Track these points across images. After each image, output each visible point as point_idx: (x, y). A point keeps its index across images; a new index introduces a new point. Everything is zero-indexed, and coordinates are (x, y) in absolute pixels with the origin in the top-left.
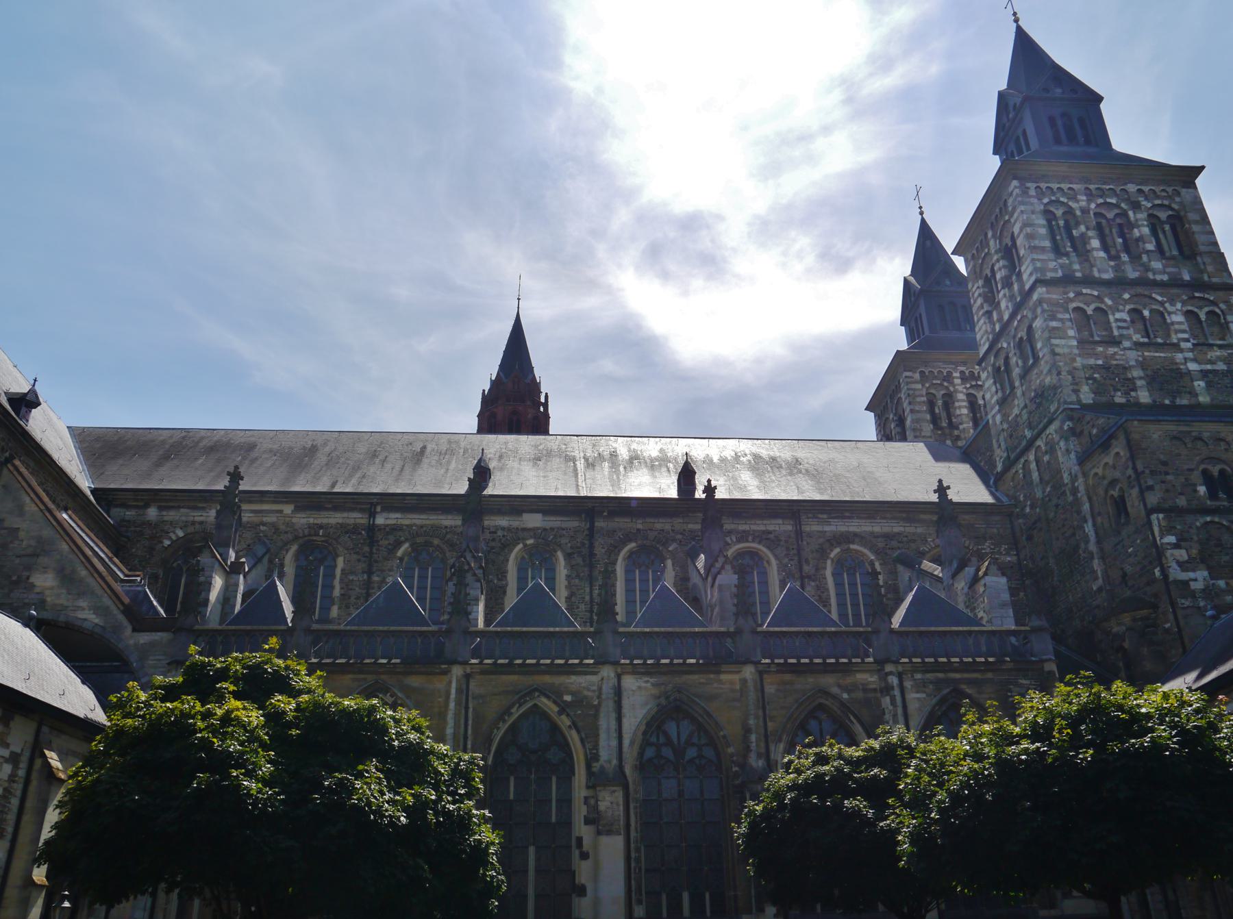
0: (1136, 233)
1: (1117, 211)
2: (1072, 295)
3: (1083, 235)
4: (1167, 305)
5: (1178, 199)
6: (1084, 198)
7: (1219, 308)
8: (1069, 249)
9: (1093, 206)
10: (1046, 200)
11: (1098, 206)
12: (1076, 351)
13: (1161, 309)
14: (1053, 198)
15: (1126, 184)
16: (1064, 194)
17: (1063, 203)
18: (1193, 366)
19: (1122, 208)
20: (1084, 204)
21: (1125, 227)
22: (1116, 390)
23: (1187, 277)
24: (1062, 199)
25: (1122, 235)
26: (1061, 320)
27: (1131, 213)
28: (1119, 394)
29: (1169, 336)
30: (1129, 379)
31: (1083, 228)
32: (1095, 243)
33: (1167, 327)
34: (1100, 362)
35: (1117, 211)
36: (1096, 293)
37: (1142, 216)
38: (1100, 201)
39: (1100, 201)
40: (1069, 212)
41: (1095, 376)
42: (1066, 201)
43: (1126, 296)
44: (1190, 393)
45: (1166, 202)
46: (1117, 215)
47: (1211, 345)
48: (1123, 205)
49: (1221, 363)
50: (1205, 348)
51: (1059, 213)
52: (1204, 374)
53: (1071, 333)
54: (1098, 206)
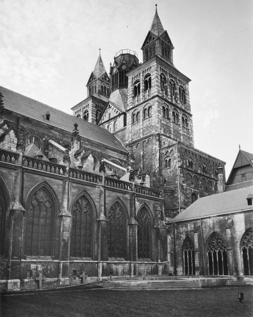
0: (176, 91)
1: (173, 83)
2: (163, 102)
3: (166, 86)
4: (179, 114)
5: (185, 86)
6: (169, 76)
7: (188, 119)
8: (163, 89)
9: (170, 79)
10: (161, 72)
11: (171, 80)
12: (162, 119)
13: (178, 114)
14: (163, 73)
15: (177, 76)
16: (165, 73)
17: (164, 75)
18: (181, 132)
19: (174, 83)
20: (168, 78)
21: (174, 88)
22: (168, 132)
23: (183, 108)
24: (164, 74)
25: (173, 91)
26: (160, 108)
27: (176, 85)
28: (168, 133)
29: (178, 122)
30: (170, 130)
31: (167, 84)
32: (169, 90)
33: (178, 119)
34: (166, 123)
35: (173, 83)
36: (168, 104)
37: (178, 87)
38: (171, 78)
39: (171, 78)
40: (165, 79)
41: (165, 127)
42: (165, 75)
43: (173, 108)
44: (180, 138)
45: (183, 86)
46: (173, 84)
47: (185, 128)
48: (175, 82)
49: (186, 133)
50: (184, 128)
51: (163, 77)
52: (183, 135)
53: (162, 113)
54: (171, 80)
